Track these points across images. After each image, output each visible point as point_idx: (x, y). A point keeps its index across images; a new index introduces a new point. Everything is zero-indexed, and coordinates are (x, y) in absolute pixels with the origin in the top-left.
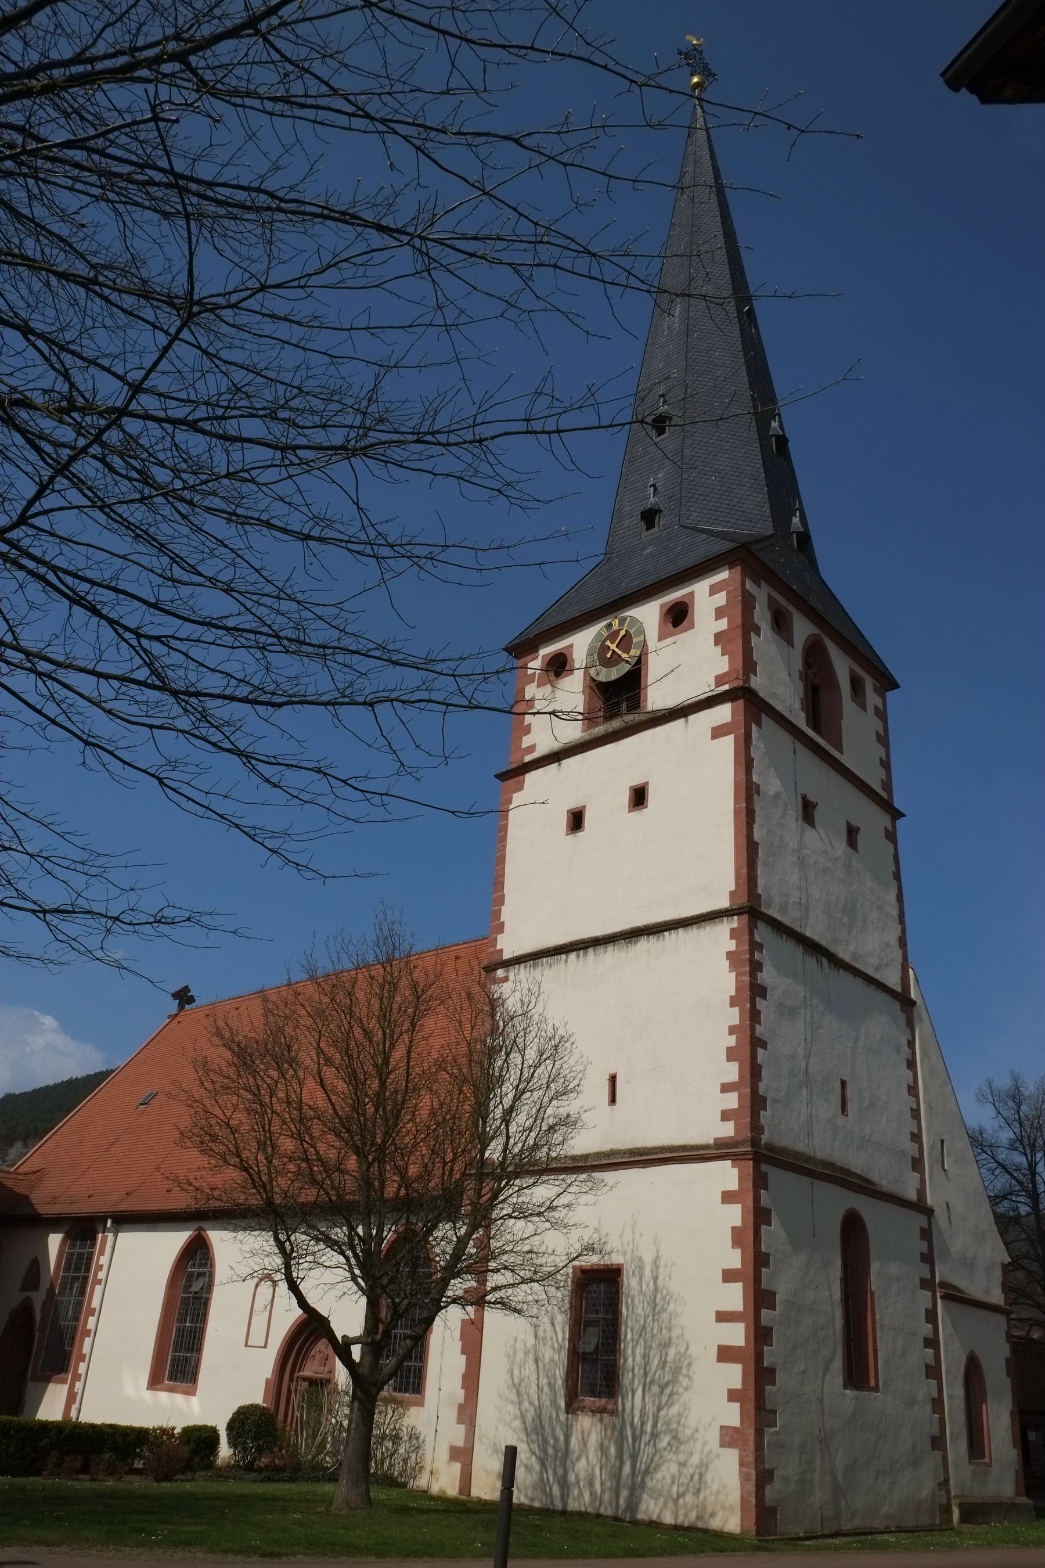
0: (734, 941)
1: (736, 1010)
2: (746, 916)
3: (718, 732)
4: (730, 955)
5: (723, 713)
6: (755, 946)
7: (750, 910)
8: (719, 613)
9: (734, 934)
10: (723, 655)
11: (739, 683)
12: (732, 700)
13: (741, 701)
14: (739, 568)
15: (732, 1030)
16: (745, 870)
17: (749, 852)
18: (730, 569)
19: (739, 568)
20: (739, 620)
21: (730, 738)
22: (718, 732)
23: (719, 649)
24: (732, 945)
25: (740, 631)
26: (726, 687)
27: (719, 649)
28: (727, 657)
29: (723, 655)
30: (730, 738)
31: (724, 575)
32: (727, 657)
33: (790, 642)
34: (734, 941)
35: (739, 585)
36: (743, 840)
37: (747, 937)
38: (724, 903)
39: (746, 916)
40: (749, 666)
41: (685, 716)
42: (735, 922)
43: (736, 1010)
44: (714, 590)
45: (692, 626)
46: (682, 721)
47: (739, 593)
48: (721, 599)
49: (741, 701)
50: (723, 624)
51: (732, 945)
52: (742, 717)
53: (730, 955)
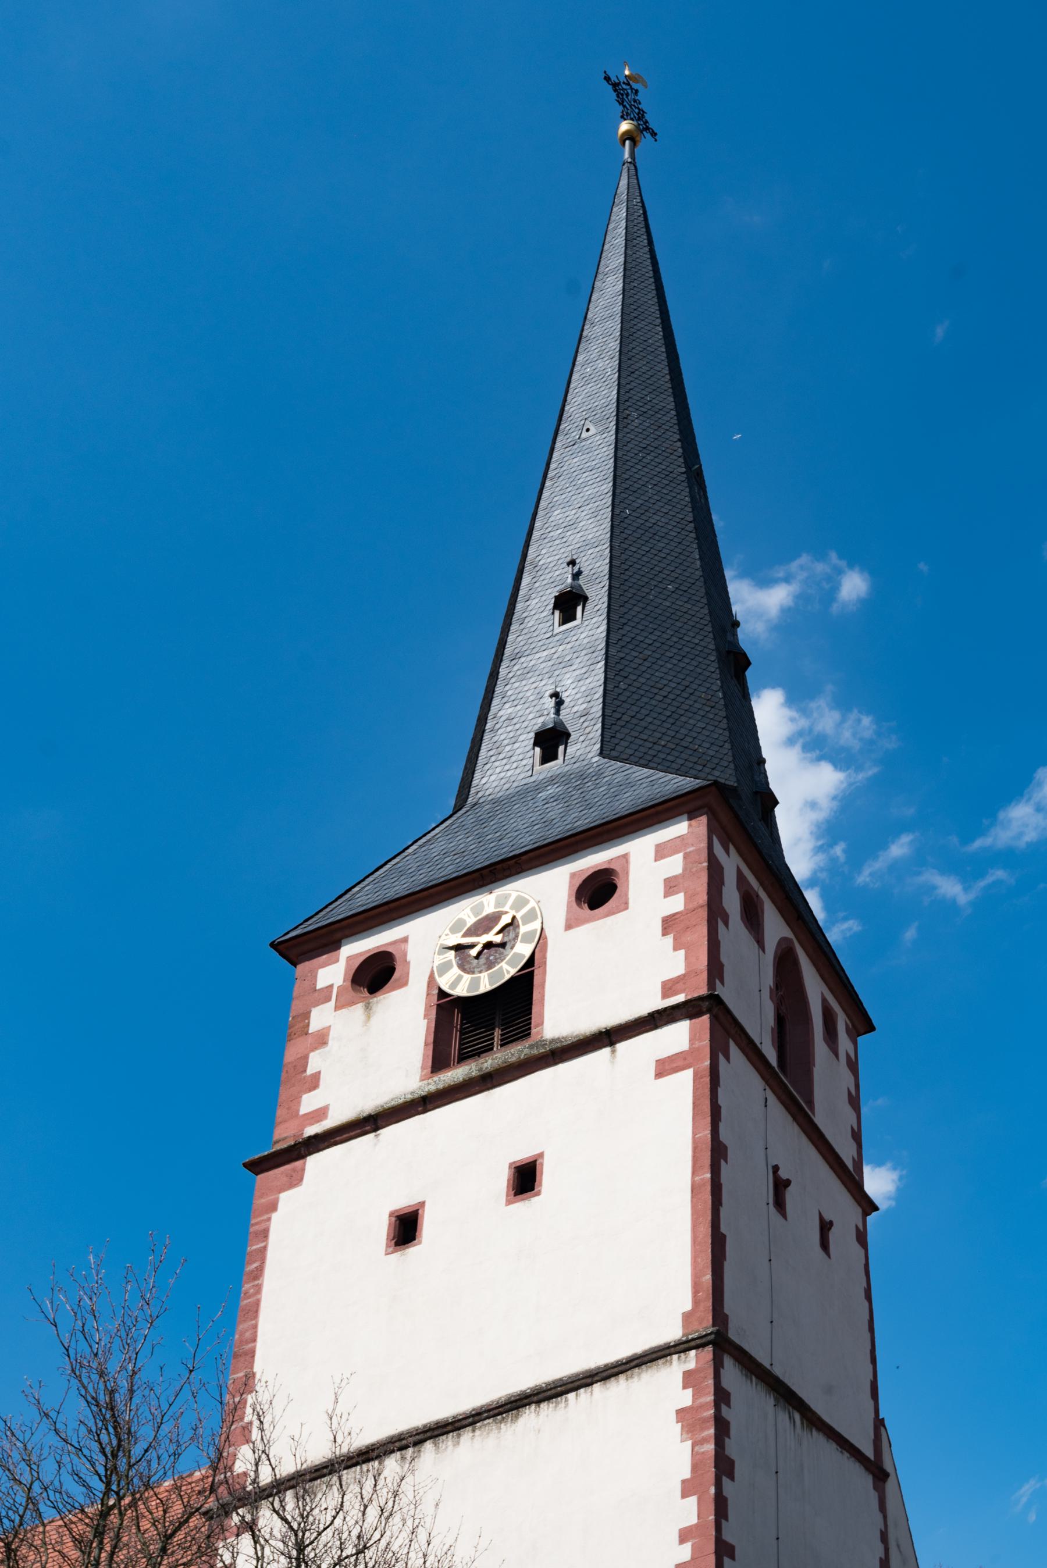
0: (689, 1392)
1: (693, 1500)
2: (710, 1349)
3: (665, 1067)
4: (682, 1414)
5: (678, 1036)
6: (722, 1397)
7: (719, 1340)
8: (671, 886)
9: (689, 1379)
10: (676, 948)
11: (703, 991)
12: (691, 1017)
13: (706, 1018)
14: (704, 819)
15: (684, 1536)
16: (708, 1277)
17: (717, 1249)
18: (690, 819)
19: (704, 819)
20: (703, 898)
21: (686, 1076)
22: (665, 1067)
23: (669, 940)
24: (686, 1398)
25: (704, 913)
26: (680, 998)
27: (669, 940)
28: (682, 952)
29: (676, 948)
30: (686, 1076)
31: (680, 828)
32: (682, 952)
33: (760, 942)
34: (689, 1392)
35: (704, 845)
36: (706, 1230)
37: (711, 1382)
38: (674, 1333)
39: (710, 1349)
40: (715, 969)
41: (612, 1044)
42: (691, 1360)
43: (693, 1500)
44: (662, 852)
45: (625, 906)
46: (606, 1051)
47: (704, 855)
48: (674, 865)
49: (706, 1018)
50: (677, 903)
51: (686, 1398)
52: (706, 1042)
53: (682, 1414)
